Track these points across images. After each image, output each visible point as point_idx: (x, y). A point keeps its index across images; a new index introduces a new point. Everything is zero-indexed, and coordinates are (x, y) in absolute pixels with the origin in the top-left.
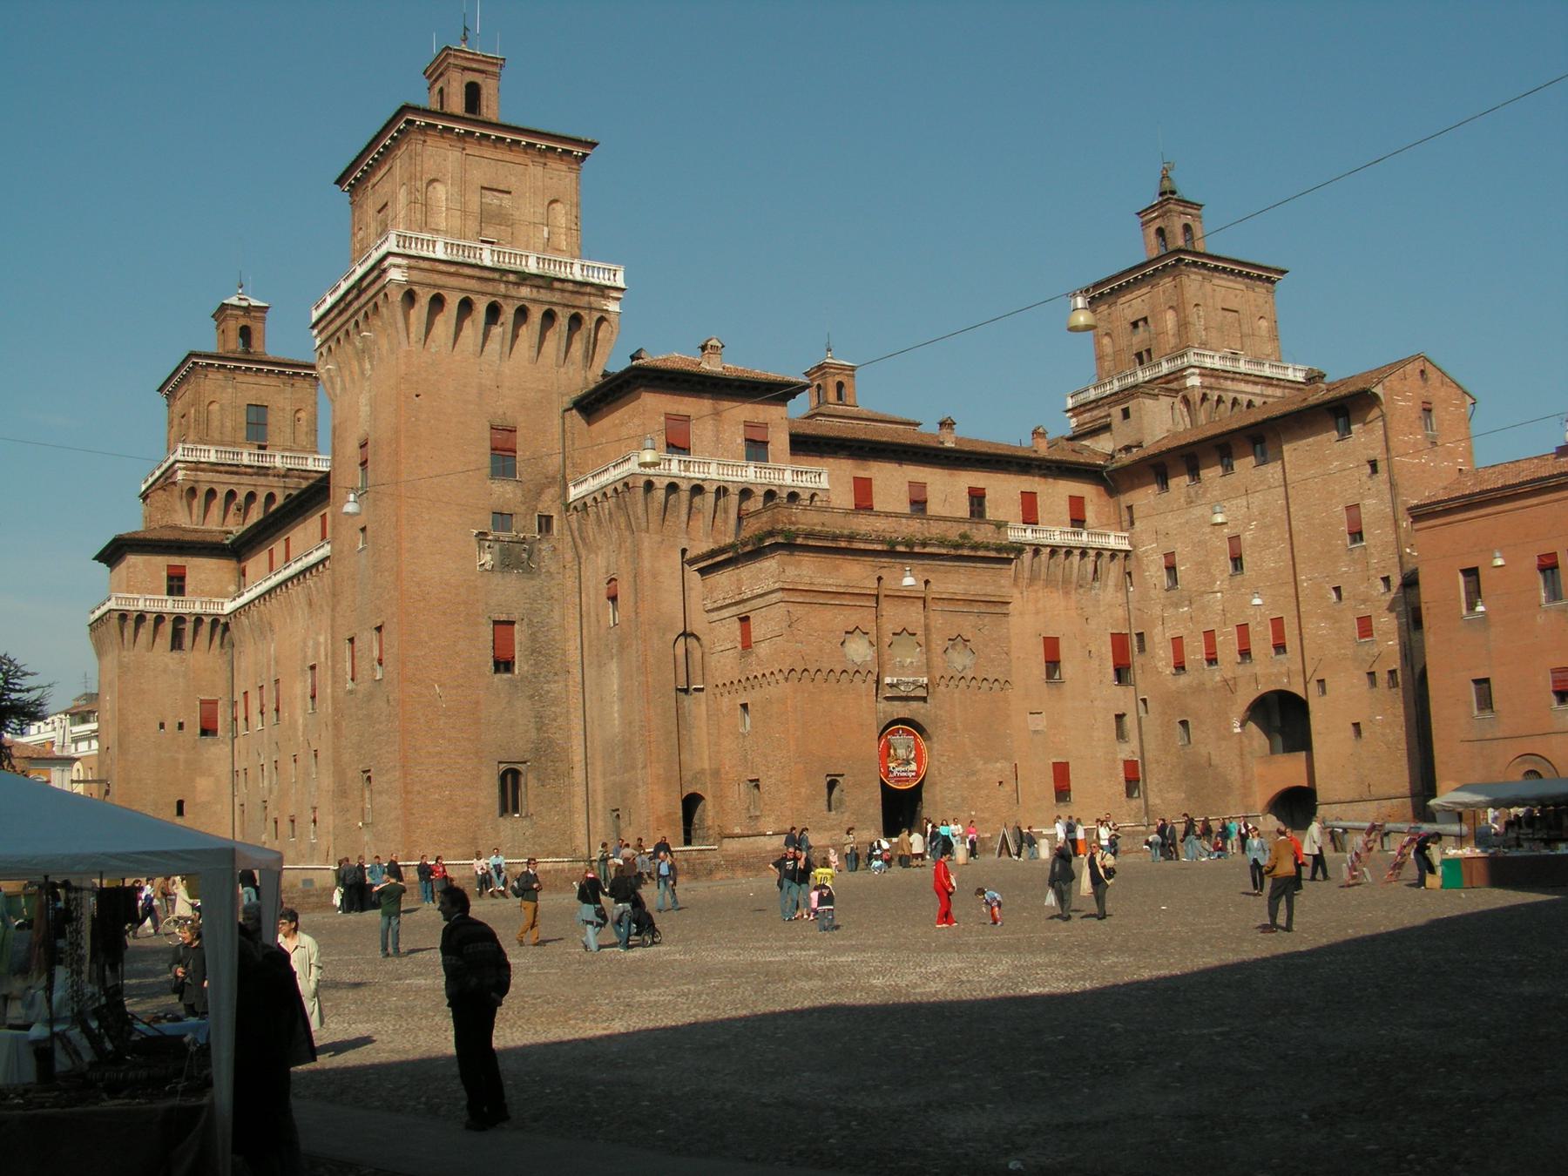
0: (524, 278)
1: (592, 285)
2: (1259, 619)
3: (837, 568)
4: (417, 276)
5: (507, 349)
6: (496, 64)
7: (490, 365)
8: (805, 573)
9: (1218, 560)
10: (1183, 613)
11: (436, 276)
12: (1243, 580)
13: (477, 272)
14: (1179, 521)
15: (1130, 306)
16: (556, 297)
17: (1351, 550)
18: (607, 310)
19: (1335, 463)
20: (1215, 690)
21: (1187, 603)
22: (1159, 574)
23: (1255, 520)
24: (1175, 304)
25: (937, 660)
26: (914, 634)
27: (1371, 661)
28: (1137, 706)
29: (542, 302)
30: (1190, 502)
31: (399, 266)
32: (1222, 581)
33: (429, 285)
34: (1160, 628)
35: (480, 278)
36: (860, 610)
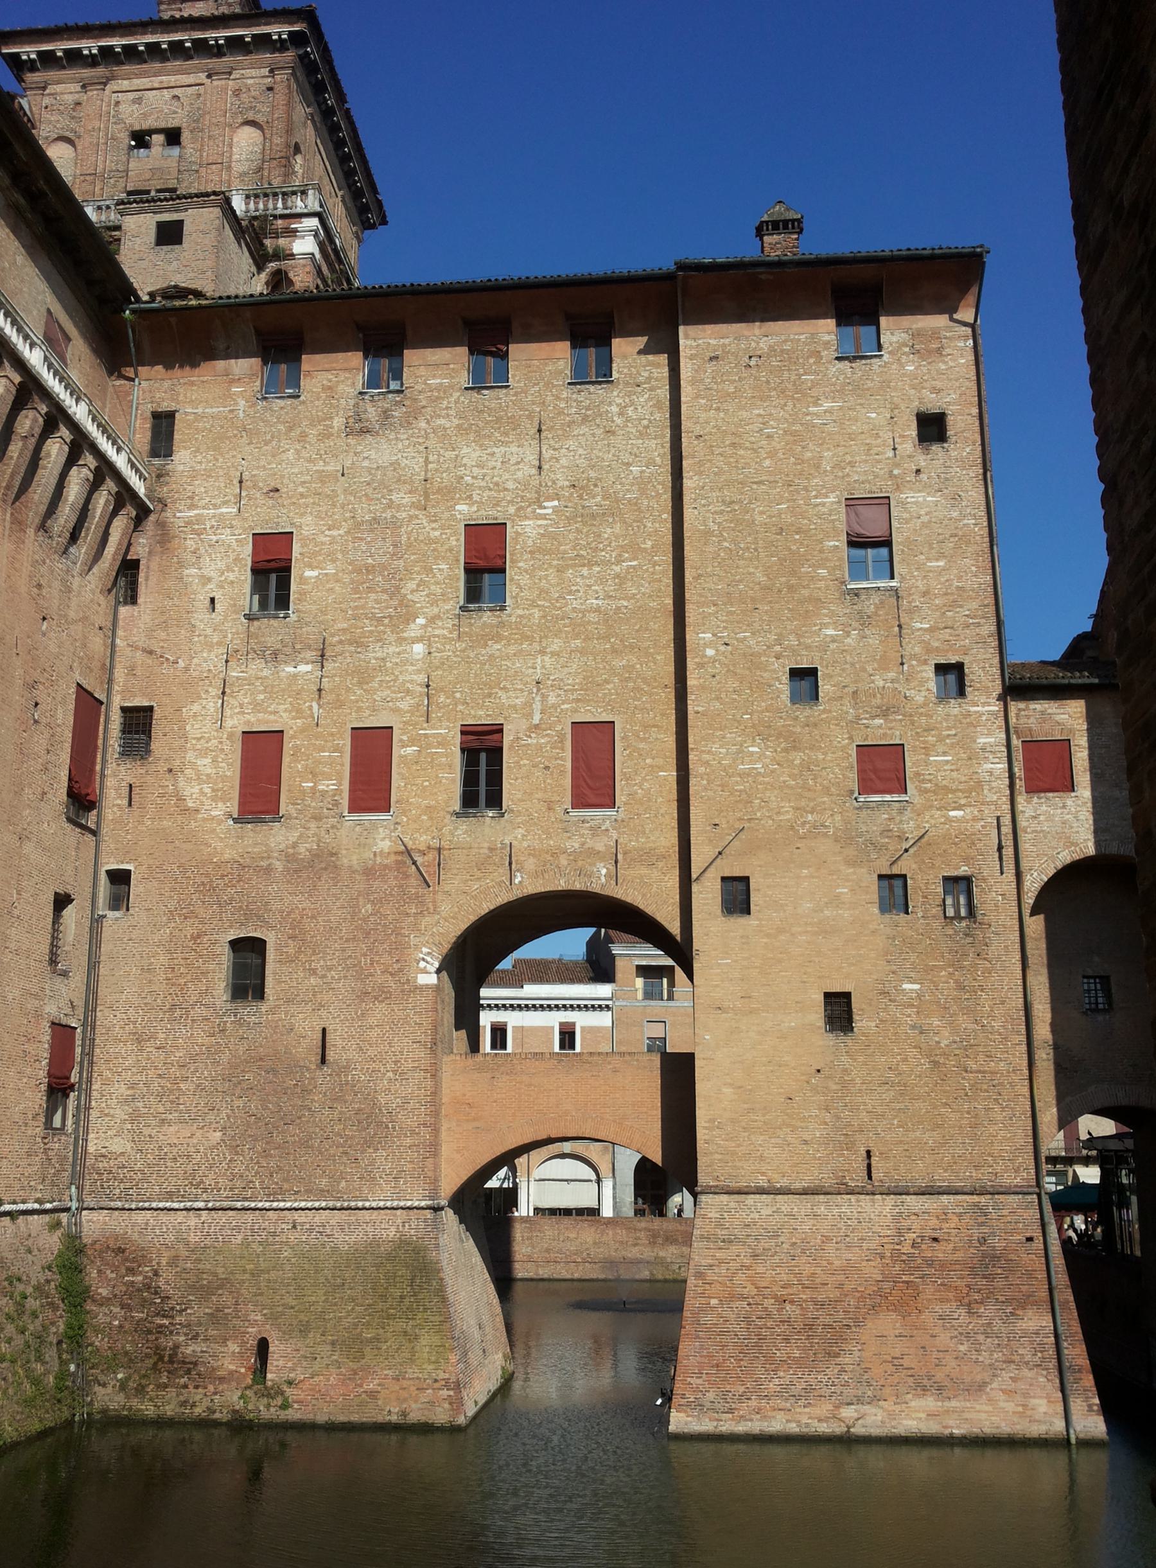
2: (536, 719)
9: (429, 570)
10: (295, 676)
12: (502, 624)
14: (320, 466)
15: (138, 101)
17: (856, 593)
19: (827, 405)
20: (369, 872)
21: (310, 655)
22: (231, 576)
23: (557, 497)
24: (260, 118)
27: (896, 847)
28: (95, 885)
30: (359, 428)
32: (432, 620)
34: (212, 705)
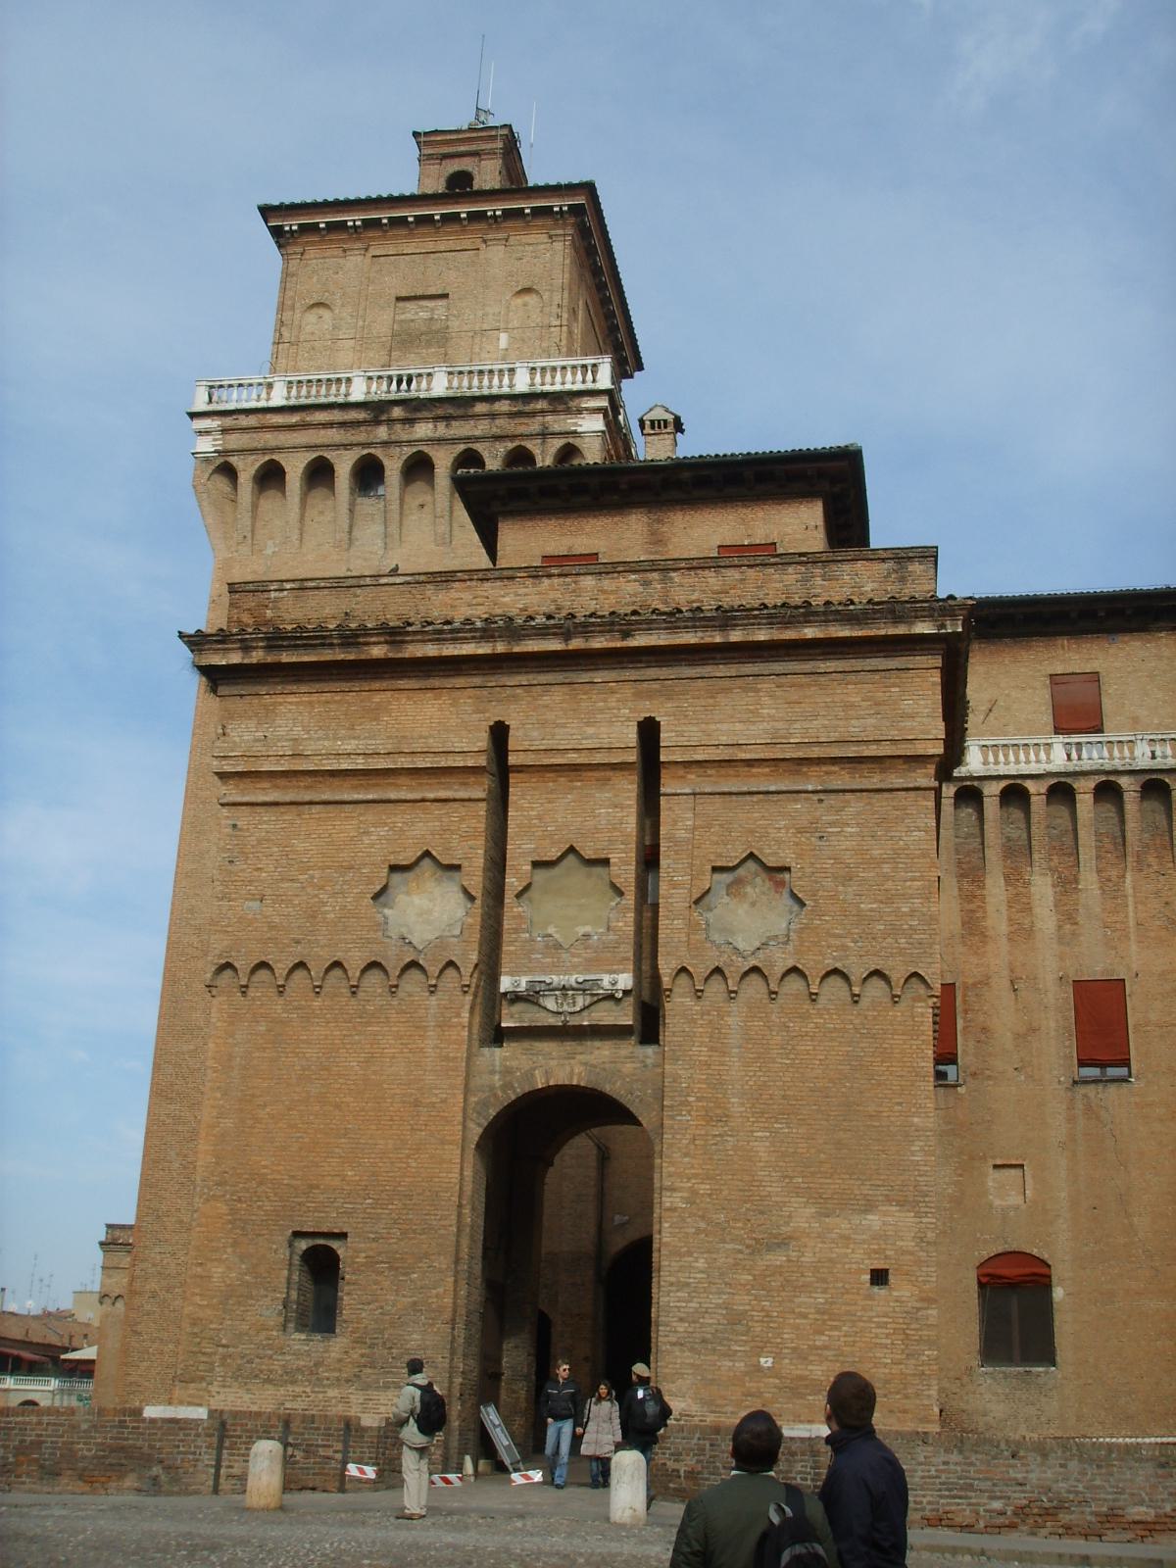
0: (417, 408)
1: (544, 395)
3: (375, 713)
4: (235, 441)
5: (393, 528)
6: (493, 138)
7: (365, 560)
8: (282, 732)
11: (268, 436)
13: (337, 416)
16: (481, 428)
18: (575, 432)
25: (671, 927)
26: (605, 862)
29: (454, 441)
31: (207, 432)
33: (253, 451)
35: (343, 424)
36: (438, 810)
